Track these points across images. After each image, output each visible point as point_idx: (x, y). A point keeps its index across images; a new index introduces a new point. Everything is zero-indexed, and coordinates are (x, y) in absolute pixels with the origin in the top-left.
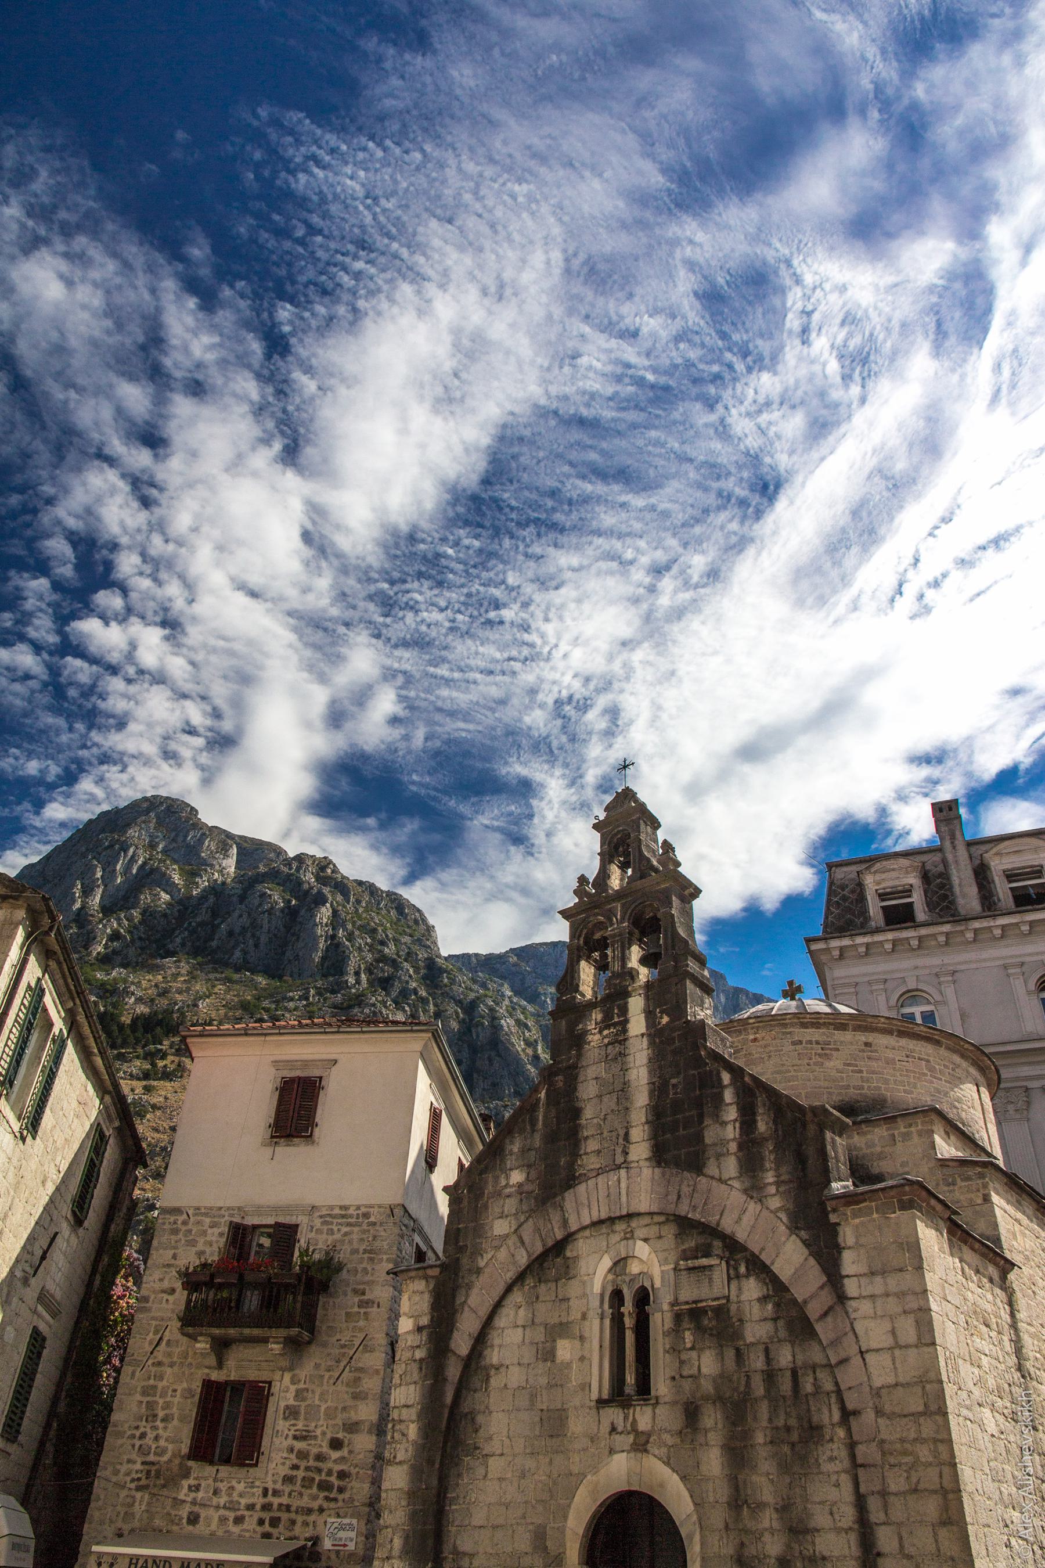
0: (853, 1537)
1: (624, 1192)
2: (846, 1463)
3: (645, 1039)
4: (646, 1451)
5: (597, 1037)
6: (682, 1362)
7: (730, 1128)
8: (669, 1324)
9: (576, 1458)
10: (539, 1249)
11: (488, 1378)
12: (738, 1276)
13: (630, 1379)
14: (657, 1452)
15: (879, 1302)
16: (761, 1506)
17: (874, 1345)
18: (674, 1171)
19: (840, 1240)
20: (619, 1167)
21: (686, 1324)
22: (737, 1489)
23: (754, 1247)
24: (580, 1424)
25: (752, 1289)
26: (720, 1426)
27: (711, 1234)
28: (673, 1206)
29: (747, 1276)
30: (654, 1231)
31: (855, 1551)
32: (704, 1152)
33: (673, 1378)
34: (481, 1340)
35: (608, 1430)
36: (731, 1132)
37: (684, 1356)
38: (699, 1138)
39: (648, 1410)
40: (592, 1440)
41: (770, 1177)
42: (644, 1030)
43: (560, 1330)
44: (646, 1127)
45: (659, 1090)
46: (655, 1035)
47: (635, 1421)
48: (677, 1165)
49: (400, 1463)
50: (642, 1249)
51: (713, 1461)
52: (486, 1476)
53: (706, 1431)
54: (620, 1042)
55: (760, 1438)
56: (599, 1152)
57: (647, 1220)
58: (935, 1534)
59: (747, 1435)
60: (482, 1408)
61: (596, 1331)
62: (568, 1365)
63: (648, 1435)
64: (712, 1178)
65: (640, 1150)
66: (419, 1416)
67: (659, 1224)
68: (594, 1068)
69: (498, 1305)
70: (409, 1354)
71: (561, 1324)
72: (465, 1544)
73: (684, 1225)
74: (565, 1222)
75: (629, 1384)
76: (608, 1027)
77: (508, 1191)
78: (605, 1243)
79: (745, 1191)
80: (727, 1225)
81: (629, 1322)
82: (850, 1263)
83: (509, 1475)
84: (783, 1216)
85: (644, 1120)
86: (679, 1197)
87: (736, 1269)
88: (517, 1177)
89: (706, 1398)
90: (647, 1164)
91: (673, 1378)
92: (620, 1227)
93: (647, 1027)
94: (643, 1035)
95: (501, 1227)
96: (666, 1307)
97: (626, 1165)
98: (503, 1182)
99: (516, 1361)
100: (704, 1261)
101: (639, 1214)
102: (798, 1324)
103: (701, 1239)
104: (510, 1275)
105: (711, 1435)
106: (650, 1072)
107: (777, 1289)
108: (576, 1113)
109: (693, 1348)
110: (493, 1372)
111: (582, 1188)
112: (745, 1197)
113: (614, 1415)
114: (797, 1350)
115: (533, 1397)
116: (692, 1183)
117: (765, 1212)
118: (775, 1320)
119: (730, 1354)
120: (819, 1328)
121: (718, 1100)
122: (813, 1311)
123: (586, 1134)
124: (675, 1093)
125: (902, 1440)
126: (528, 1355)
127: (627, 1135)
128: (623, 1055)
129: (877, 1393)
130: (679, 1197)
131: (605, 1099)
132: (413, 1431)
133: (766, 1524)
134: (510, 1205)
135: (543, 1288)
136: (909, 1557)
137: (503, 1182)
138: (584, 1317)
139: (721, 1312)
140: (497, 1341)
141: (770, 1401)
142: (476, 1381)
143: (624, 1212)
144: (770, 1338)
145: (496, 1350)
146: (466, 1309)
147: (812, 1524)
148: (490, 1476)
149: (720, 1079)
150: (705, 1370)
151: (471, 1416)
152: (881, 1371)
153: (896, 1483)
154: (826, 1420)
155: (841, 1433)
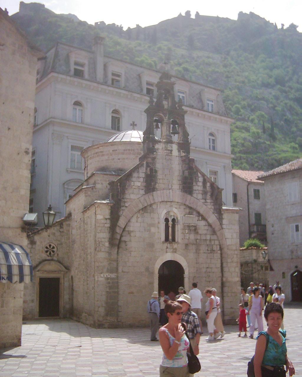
4: (176, 253)
6: (185, 236)
7: (200, 187)
10: (146, 205)
12: (199, 220)
13: (170, 237)
14: (178, 253)
18: (185, 194)
19: (223, 217)
20: (170, 189)
21: (186, 228)
25: (203, 223)
29: (201, 220)
35: (166, 248)
37: (185, 235)
41: (209, 201)
42: (178, 155)
48: (186, 193)
49: (103, 252)
50: (175, 210)
51: (192, 255)
52: (130, 256)
55: (202, 251)
57: (177, 203)
60: (128, 240)
64: (195, 198)
65: (176, 185)
67: (180, 205)
74: (154, 199)
75: (170, 238)
77: (134, 187)
82: (225, 222)
86: (186, 200)
87: (199, 219)
91: (183, 239)
92: (169, 203)
101: (175, 202)
102: (214, 232)
103: (191, 210)
111: (159, 192)
112: (202, 204)
113: (169, 245)
125: (231, 254)
129: (228, 246)
135: (145, 214)
138: (159, 223)
146: (122, 216)
152: (229, 242)
153: (229, 260)
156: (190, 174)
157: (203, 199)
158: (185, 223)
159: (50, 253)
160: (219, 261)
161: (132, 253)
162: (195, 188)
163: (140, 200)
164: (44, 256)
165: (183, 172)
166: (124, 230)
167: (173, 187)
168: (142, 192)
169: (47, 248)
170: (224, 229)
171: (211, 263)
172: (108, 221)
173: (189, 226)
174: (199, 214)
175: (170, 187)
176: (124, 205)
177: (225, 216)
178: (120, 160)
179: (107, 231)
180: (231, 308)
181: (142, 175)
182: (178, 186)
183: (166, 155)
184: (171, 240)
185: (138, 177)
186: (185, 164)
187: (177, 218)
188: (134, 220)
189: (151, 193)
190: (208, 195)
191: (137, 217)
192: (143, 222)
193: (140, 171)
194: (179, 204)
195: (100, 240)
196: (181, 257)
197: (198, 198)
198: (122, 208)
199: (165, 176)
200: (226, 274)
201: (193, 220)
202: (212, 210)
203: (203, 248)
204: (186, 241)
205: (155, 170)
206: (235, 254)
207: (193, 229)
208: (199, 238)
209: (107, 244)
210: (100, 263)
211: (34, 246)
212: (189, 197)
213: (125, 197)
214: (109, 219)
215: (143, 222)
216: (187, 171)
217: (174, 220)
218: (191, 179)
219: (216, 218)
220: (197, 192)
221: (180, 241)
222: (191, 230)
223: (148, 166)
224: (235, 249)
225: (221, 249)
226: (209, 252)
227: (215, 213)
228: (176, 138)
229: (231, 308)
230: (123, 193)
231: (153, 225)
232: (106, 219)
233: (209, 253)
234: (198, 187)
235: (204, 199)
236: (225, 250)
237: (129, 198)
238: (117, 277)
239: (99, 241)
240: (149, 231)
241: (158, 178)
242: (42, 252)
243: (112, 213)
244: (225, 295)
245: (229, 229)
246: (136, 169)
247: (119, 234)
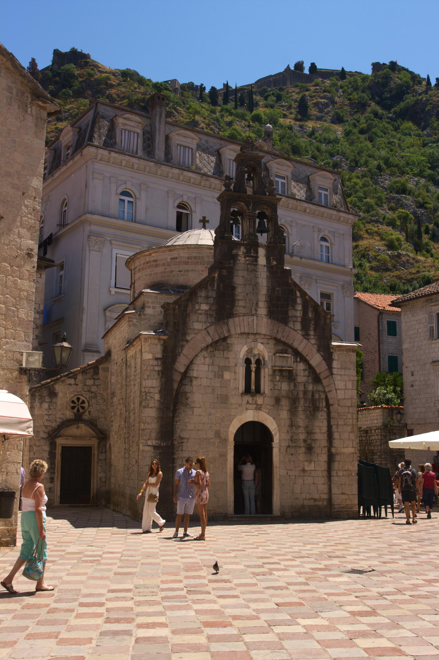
0: (326, 435)
1: (255, 324)
2: (326, 417)
3: (265, 267)
5: (243, 259)
6: (275, 385)
7: (299, 312)
8: (271, 372)
10: (217, 338)
11: (191, 381)
12: (297, 362)
13: (253, 387)
15: (343, 376)
16: (300, 426)
17: (340, 388)
19: (333, 357)
20: (253, 315)
21: (277, 373)
22: (292, 422)
23: (305, 354)
24: (235, 400)
25: (301, 366)
26: (287, 404)
29: (300, 362)
30: (265, 341)
31: (326, 438)
34: (188, 368)
36: (299, 314)
38: (286, 313)
39: (262, 398)
40: (239, 405)
43: (226, 368)
44: (265, 303)
45: (271, 290)
46: (269, 266)
49: (151, 407)
50: (261, 347)
51: (285, 414)
53: (282, 406)
54: (254, 265)
55: (300, 409)
56: (245, 307)
57: (263, 337)
58: (349, 435)
59: (296, 408)
60: (190, 391)
61: (241, 370)
62: (229, 380)
63: (262, 405)
65: (263, 310)
66: (160, 392)
68: (242, 272)
69: (196, 356)
71: (226, 366)
72: (184, 435)
73: (278, 341)
74: (229, 331)
76: (248, 256)
77: (200, 312)
78: (245, 341)
79: (303, 335)
80: (296, 345)
81: (253, 369)
82: (335, 364)
83: (204, 414)
84: (316, 346)
85: (264, 300)
86: (278, 332)
87: (296, 359)
88: (204, 307)
89: (283, 396)
90: (265, 317)
92: (252, 337)
93: (267, 263)
94: (264, 266)
95: (197, 326)
96: (269, 367)
97: (256, 315)
98: (197, 308)
99: (205, 376)
100: (286, 355)
104: (203, 345)
105: (284, 408)
106: (268, 282)
107: (311, 368)
108: (233, 289)
109: (279, 381)
110: (194, 379)
111: (237, 319)
114: (314, 386)
115: (213, 390)
117: (309, 344)
118: (308, 376)
119: (292, 384)
120: (324, 381)
121: (295, 302)
122: (322, 376)
123: (238, 298)
124: (278, 294)
126: (211, 375)
127: (257, 304)
128: (255, 271)
129: (339, 400)
130: (278, 332)
131: (247, 286)
132: (157, 397)
133: (300, 431)
134: (202, 318)
135: (217, 353)
136: (342, 439)
137: (197, 308)
139: (290, 372)
141: (305, 399)
142: (186, 381)
143: (255, 332)
144: (306, 382)
145: (195, 372)
146: (182, 355)
147: (314, 432)
148: (194, 414)
149: (296, 294)
150: (283, 388)
151: (186, 393)
152: (341, 395)
153: (341, 422)
154: (321, 405)
155: (325, 409)
158: (274, 366)
159: (78, 410)
160: (325, 423)
161: (195, 409)
162: (291, 313)
163: (208, 332)
164: (69, 414)
169: (73, 402)
170: (334, 376)
173: (281, 371)
174: (297, 354)
175: (254, 312)
177: (335, 356)
178: (182, 273)
179: (156, 376)
183: (249, 264)
184: (254, 391)
187: (264, 359)
188: (199, 360)
189: (226, 321)
191: (205, 358)
192: (213, 364)
194: (267, 337)
195: (147, 390)
197: (296, 329)
199: (247, 295)
200: (336, 443)
201: (289, 361)
206: (348, 412)
207: (287, 374)
210: (146, 424)
211: (54, 400)
215: (213, 364)
217: (258, 362)
221: (267, 392)
225: (328, 405)
228: (263, 239)
229: (343, 493)
238: (173, 445)
239: (145, 392)
240: (222, 376)
242: (66, 408)
243: (165, 350)
244: (334, 473)
245: (341, 375)
246: (202, 285)
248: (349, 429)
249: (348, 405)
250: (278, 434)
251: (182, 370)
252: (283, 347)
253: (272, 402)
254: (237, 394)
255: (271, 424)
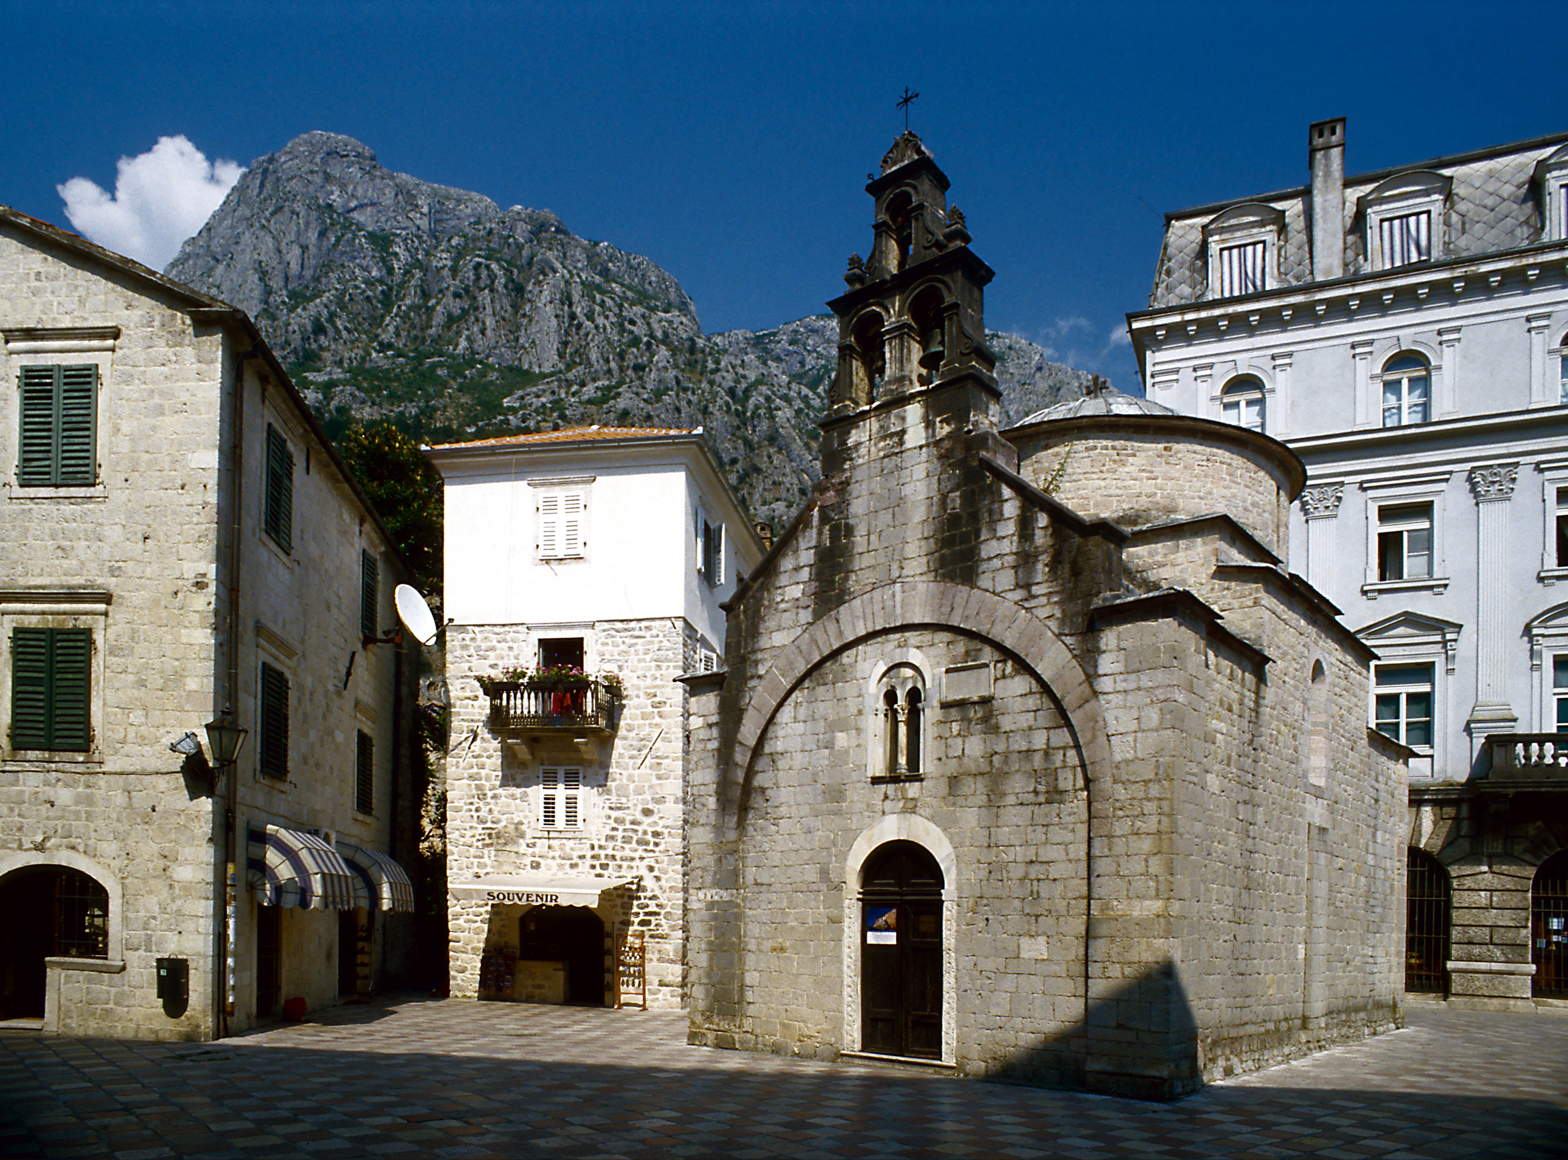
4: (914, 813)
9: (854, 819)
12: (1004, 677)
20: (894, 582)
24: (860, 794)
27: (981, 641)
28: (946, 617)
32: (978, 567)
33: (940, 759)
44: (923, 542)
47: (904, 791)
48: (952, 580)
66: (716, 792)
70: (702, 746)
80: (998, 633)
86: (952, 609)
90: (924, 578)
91: (940, 759)
96: (936, 703)
99: (799, 748)
109: (959, 735)
116: (965, 596)
130: (952, 609)
138: (860, 712)
140: (781, 733)
156: (969, 499)
157: (1018, 586)
162: (988, 549)
165: (944, 498)
166: (757, 751)
167: (905, 572)
168: (806, 616)
171: (1046, 843)
172: (715, 732)
174: (1006, 653)
175: (895, 573)
176: (754, 671)
180: (1119, 1026)
181: (807, 556)
182: (924, 560)
185: (797, 569)
186: (949, 465)
190: (1040, 566)
193: (803, 545)
196: (932, 826)
198: (752, 683)
200: (1104, 887)
202: (1053, 624)
203: (1018, 785)
204: (952, 767)
205: (847, 524)
208: (1001, 747)
209: (712, 803)
212: (964, 590)
213: (756, 647)
214: (717, 724)
216: (958, 493)
218: (974, 518)
219: (1070, 656)
220: (997, 563)
222: (970, 721)
223: (824, 519)
224: (1152, 776)
226: (1042, 799)
227: (1066, 635)
229: (1119, 1026)
230: (754, 633)
231: (840, 725)
232: (710, 726)
233: (1040, 804)
234: (1000, 544)
235: (1021, 587)
236: (1105, 784)
237: (768, 646)
241: (855, 551)
247: (741, 767)
248: (1146, 845)
249: (1146, 778)
250: (954, 870)
251: (752, 742)
252: (975, 642)
253: (944, 789)
254: (864, 779)
255: (941, 849)
